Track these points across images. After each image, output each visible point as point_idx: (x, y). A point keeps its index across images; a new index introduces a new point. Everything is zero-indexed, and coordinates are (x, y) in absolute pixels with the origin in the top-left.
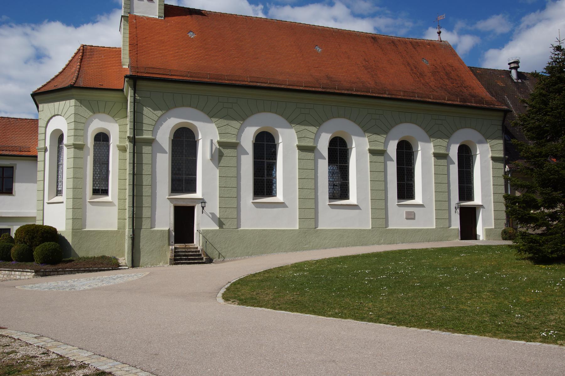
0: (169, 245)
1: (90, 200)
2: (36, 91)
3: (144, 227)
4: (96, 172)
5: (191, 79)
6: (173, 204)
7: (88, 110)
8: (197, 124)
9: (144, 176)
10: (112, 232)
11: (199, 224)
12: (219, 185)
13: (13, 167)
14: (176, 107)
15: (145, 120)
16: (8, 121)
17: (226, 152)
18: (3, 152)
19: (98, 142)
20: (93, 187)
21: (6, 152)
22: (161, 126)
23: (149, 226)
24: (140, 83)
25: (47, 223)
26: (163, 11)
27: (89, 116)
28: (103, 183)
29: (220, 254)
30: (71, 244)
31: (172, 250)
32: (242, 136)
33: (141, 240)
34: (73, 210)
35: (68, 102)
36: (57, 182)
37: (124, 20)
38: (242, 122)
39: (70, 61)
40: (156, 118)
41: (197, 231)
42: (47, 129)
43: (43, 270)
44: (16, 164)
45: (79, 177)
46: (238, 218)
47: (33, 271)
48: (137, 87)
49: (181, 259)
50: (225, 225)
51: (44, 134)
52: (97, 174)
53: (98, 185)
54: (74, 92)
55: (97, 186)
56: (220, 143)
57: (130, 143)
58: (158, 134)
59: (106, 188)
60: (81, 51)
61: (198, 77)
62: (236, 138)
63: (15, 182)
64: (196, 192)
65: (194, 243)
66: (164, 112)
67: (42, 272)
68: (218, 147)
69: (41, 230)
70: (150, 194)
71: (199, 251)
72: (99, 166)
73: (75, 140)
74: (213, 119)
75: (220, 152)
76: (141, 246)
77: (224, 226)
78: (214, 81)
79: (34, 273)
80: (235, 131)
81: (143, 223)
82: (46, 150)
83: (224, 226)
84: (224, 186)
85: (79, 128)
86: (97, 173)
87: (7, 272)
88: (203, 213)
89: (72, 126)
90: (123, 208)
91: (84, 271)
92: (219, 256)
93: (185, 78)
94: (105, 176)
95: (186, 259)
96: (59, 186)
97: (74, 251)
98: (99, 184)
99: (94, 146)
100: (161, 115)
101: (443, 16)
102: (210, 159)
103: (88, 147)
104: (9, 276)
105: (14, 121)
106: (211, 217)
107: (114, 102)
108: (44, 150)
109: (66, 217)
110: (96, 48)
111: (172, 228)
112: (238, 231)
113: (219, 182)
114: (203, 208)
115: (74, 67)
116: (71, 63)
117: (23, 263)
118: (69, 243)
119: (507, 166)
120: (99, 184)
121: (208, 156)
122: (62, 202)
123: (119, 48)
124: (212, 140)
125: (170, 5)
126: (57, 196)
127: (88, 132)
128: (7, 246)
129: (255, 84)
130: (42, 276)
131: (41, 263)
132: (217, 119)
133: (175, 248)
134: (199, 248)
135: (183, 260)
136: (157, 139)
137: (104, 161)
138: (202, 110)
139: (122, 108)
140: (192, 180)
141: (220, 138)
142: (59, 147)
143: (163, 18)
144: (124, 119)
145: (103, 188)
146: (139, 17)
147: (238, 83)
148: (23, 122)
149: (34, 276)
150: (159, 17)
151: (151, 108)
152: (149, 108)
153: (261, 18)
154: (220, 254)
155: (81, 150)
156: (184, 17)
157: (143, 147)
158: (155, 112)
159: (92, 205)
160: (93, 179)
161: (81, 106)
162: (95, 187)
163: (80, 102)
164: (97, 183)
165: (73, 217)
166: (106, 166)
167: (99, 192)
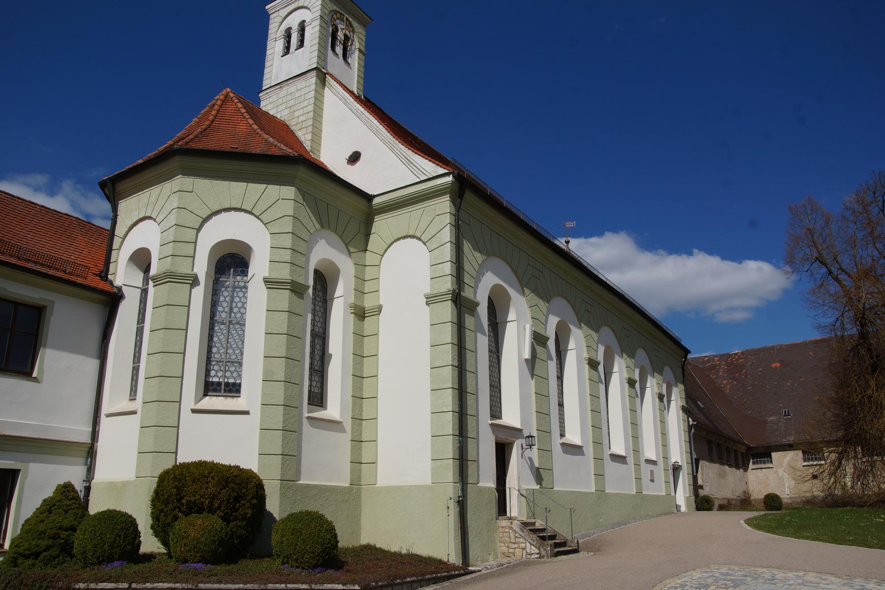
8: (512, 292)
10: (342, 489)
15: (467, 266)
43: (374, 584)
44: (53, 303)
45: (293, 358)
54: (302, 172)
63: (45, 346)
64: (501, 417)
73: (292, 272)
82: (195, 282)
85: (298, 249)
96: (213, 373)
101: (572, 223)
102: (526, 360)
108: (191, 282)
119: (690, 419)
122: (247, 413)
126: (205, 395)
144: (362, 254)
152: (470, 245)
161: (303, 204)
163: (302, 196)
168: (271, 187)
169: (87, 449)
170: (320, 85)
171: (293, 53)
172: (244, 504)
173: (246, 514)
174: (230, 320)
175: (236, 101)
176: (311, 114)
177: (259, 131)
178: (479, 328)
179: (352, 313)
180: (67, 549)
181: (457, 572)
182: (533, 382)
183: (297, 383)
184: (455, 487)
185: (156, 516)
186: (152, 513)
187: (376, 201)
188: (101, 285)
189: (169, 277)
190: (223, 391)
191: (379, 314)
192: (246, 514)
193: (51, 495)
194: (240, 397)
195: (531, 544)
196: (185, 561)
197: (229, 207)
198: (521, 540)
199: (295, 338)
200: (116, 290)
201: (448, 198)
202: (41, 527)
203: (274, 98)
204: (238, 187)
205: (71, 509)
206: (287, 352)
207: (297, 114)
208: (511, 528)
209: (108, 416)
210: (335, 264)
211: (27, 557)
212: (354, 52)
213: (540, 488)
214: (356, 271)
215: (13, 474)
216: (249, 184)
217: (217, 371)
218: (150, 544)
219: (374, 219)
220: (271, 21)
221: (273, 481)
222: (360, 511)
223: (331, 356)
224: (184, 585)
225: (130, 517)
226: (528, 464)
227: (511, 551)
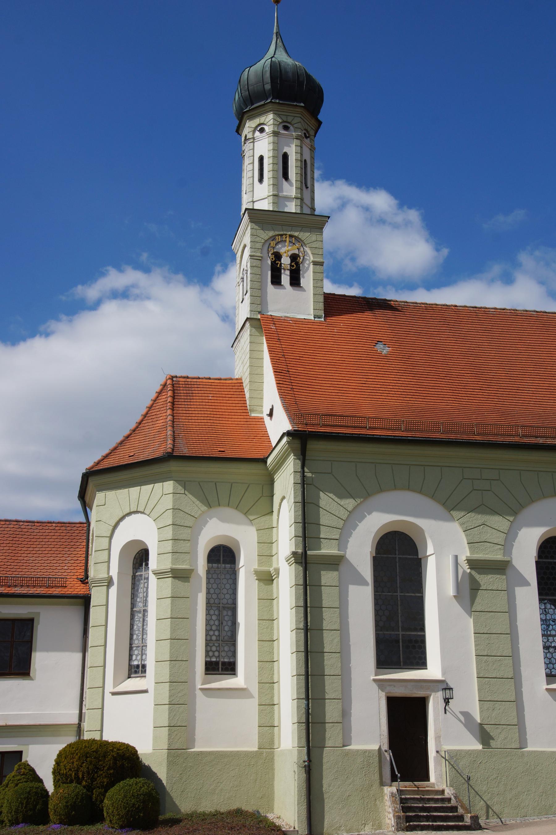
0: (382, 784)
1: (202, 685)
2: (92, 467)
3: (329, 743)
4: (211, 626)
5: (409, 434)
6: (384, 693)
7: (198, 502)
9: (325, 634)
10: (247, 754)
11: (440, 737)
12: (476, 650)
13: (31, 621)
14: (381, 490)
15: (324, 519)
16: (17, 526)
17: (484, 580)
18: (16, 589)
19: (214, 565)
20: (206, 657)
21: (21, 589)
22: (354, 530)
23: (339, 742)
24: (313, 446)
25: (110, 736)
26: (321, 306)
27: (200, 512)
28: (226, 648)
29: (488, 807)
30: (164, 782)
31: (392, 795)
32: (514, 547)
33: (324, 773)
34: (170, 708)
35: (158, 486)
36: (131, 648)
37: (251, 326)
38: (511, 519)
39: (150, 408)
40: (344, 515)
41: (437, 752)
42: (113, 541)
44: (39, 613)
45: (180, 637)
46: (520, 725)
49: (418, 818)
50: (493, 739)
51: (107, 552)
52: (214, 631)
53: (216, 654)
54: (173, 466)
55: (214, 655)
56: (470, 562)
57: (297, 566)
58: (349, 545)
59: (231, 660)
60: (169, 387)
61: (422, 431)
62: (502, 551)
63: (35, 651)
64: (426, 666)
65: (429, 781)
66: (359, 502)
68: (469, 571)
69: (112, 750)
70: (338, 672)
71: (449, 800)
72: (217, 613)
73: (174, 561)
74: (454, 513)
75: (473, 580)
76: (325, 787)
77: (491, 741)
78: (452, 437)
80: (500, 538)
81: (328, 735)
82: (109, 582)
83: (491, 741)
84: (485, 654)
85: (181, 537)
86: (214, 628)
88: (445, 713)
89: (169, 533)
90: (268, 702)
92: (487, 812)
93: (397, 433)
94: (229, 634)
95: (427, 818)
96: (134, 657)
97: (171, 798)
98: (217, 651)
99: (208, 572)
100: (355, 508)
102: (454, 596)
103: (198, 574)
105: (30, 527)
106: (464, 722)
107: (247, 483)
108: (106, 584)
109: (154, 723)
110: (195, 380)
111: (386, 747)
112: (523, 754)
114: (447, 701)
115: (161, 418)
116: (151, 412)
117: (77, 827)
118: (161, 781)
120: (217, 651)
121: (451, 590)
122: (146, 691)
123: (237, 379)
124: (456, 557)
125: (330, 294)
126: (129, 677)
127: (199, 545)
128: (34, 790)
129: (533, 440)
131: (122, 827)
132: (463, 513)
133: (400, 792)
134: (449, 793)
135: (421, 819)
136: (348, 556)
137: (227, 603)
138: (433, 497)
139: (262, 496)
140: (416, 641)
141: (472, 551)
142: (134, 577)
143: (323, 319)
144: (267, 517)
145: (226, 660)
146: (279, 319)
147: (500, 439)
148: (44, 528)
150: (315, 318)
151: (335, 495)
152: (331, 495)
153: (504, 309)
154: (488, 807)
155: (185, 582)
156: (359, 315)
157: (322, 572)
158: (343, 502)
159: (208, 696)
160: (206, 640)
161: (184, 494)
162: (211, 657)
163: (182, 486)
164: (214, 649)
165: (169, 723)
166: (230, 613)
167: (138, 670)
172: (102, 775)
173: (103, 782)
174: (144, 609)
183: (184, 660)
184: (299, 752)
192: (103, 782)
194: (145, 676)
197: (129, 512)
199: (181, 620)
206: (171, 634)
210: (227, 536)
213: (483, 748)
214: (258, 537)
216: (142, 487)
217: (137, 656)
221: (163, 751)
222: (273, 775)
223: (239, 624)
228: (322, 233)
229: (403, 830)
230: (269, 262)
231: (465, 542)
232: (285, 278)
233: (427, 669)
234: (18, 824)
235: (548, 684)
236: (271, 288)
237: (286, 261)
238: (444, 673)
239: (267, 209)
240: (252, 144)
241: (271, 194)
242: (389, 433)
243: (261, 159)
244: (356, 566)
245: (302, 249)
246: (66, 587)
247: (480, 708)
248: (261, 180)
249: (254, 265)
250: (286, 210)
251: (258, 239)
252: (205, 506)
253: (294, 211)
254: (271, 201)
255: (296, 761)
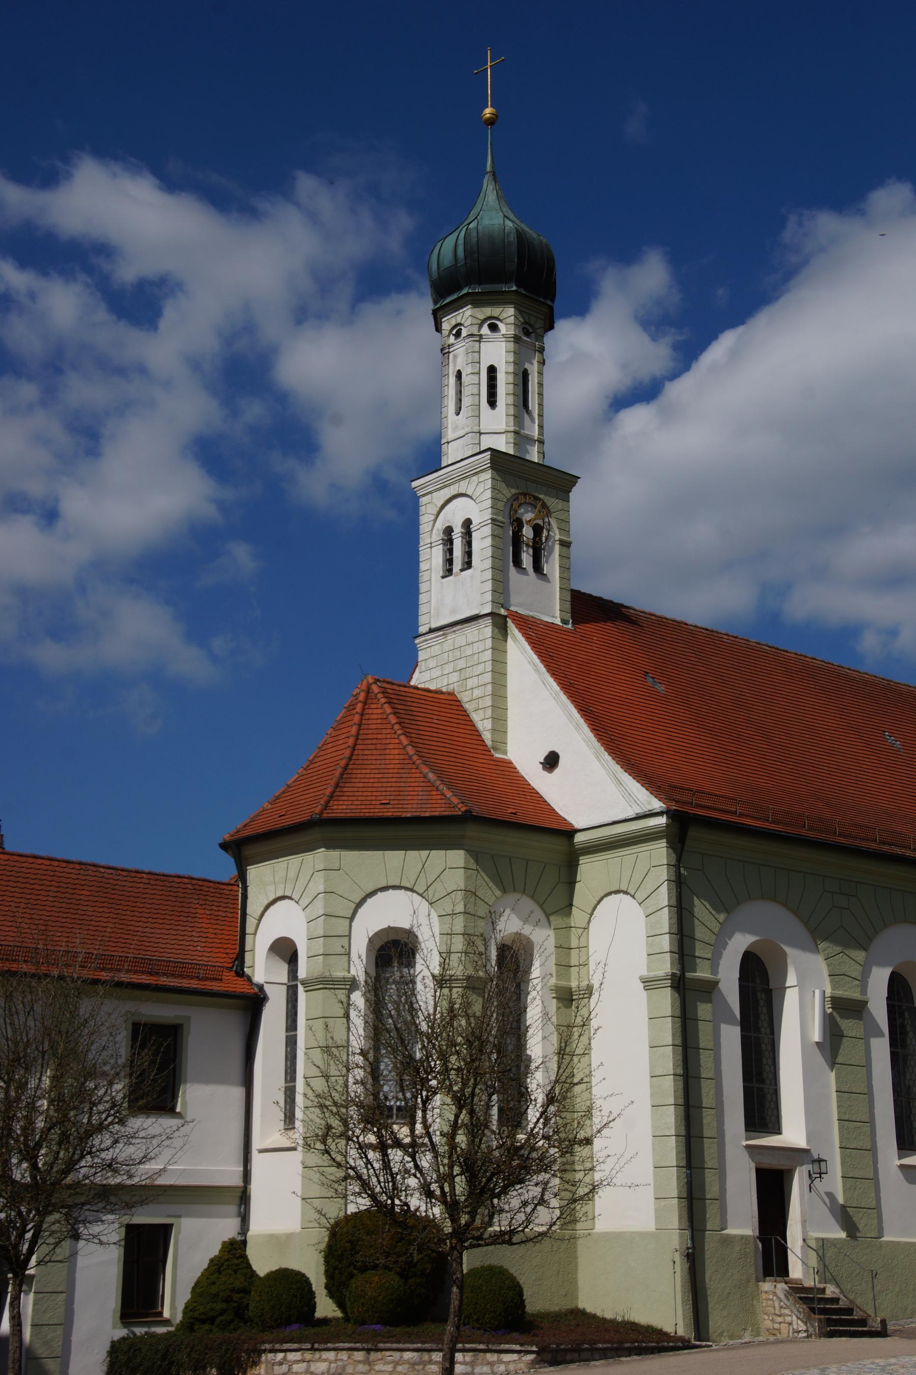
0: (758, 1280)
11: (805, 1221)
15: (700, 933)
17: (847, 1025)
26: (568, 606)
37: (494, 624)
41: (804, 1240)
42: (353, 924)
43: (554, 1346)
44: (188, 1018)
47: (534, 1349)
48: (688, 842)
54: (471, 831)
67: (552, 1351)
71: (836, 1300)
76: (707, 1280)
79: (531, 1357)
80: (856, 971)
87: (407, 1355)
88: (810, 1191)
89: (459, 925)
91: (630, 1352)
102: (817, 1043)
104: (417, 1367)
108: (348, 987)
111: (757, 1233)
113: (839, 1107)
130: (551, 1365)
141: (833, 989)
143: (570, 626)
149: (533, 1363)
153: (736, 637)
161: (477, 870)
163: (473, 859)
168: (434, 853)
169: (240, 1194)
170: (500, 637)
171: (457, 575)
175: (383, 700)
176: (489, 688)
177: (415, 758)
178: (722, 1015)
179: (554, 998)
180: (240, 1314)
181: (671, 1344)
182: (833, 1075)
184: (681, 1236)
185: (330, 1274)
186: (326, 1271)
187: (579, 838)
188: (239, 986)
189: (324, 983)
190: (395, 1117)
191: (590, 998)
193: (217, 1253)
195: (798, 1318)
196: (364, 1323)
198: (787, 1311)
200: (256, 990)
201: (665, 844)
202: (214, 1289)
203: (436, 650)
204: (395, 857)
205: (239, 1269)
207: (471, 683)
208: (775, 1294)
209: (261, 1151)
211: (203, 1322)
212: (551, 551)
215: (164, 1231)
218: (325, 1307)
219: (579, 861)
220: (422, 510)
224: (364, 1345)
225: (304, 1275)
226: (825, 1203)
227: (776, 1326)
228: (567, 500)
229: (825, 1336)
230: (511, 532)
231: (825, 972)
232: (527, 559)
233: (780, 1133)
234: (290, 1325)
235: (900, 1158)
236: (512, 570)
237: (527, 532)
238: (808, 1141)
239: (504, 450)
240: (478, 343)
241: (512, 429)
242: (788, 829)
243: (492, 370)
244: (726, 996)
245: (546, 520)
246: (221, 980)
247: (844, 1187)
248: (492, 403)
249: (496, 533)
250: (528, 457)
251: (499, 496)
252: (500, 890)
253: (536, 461)
254: (512, 441)
255: (678, 1248)
